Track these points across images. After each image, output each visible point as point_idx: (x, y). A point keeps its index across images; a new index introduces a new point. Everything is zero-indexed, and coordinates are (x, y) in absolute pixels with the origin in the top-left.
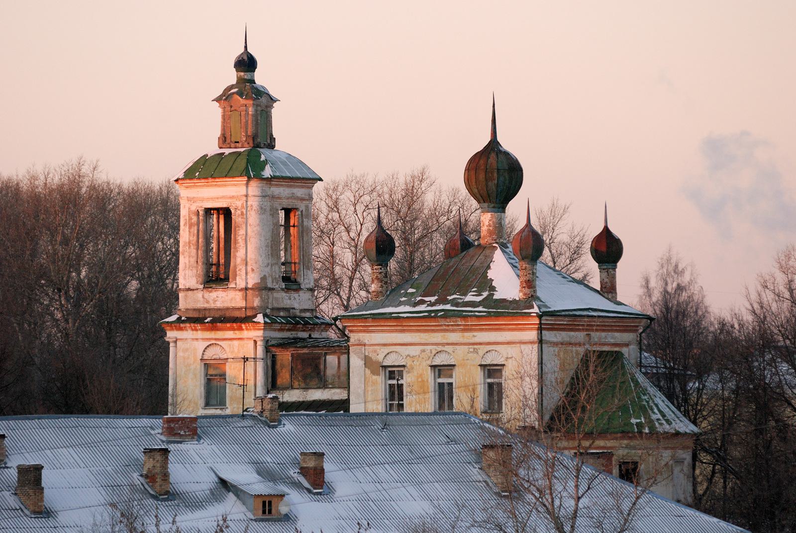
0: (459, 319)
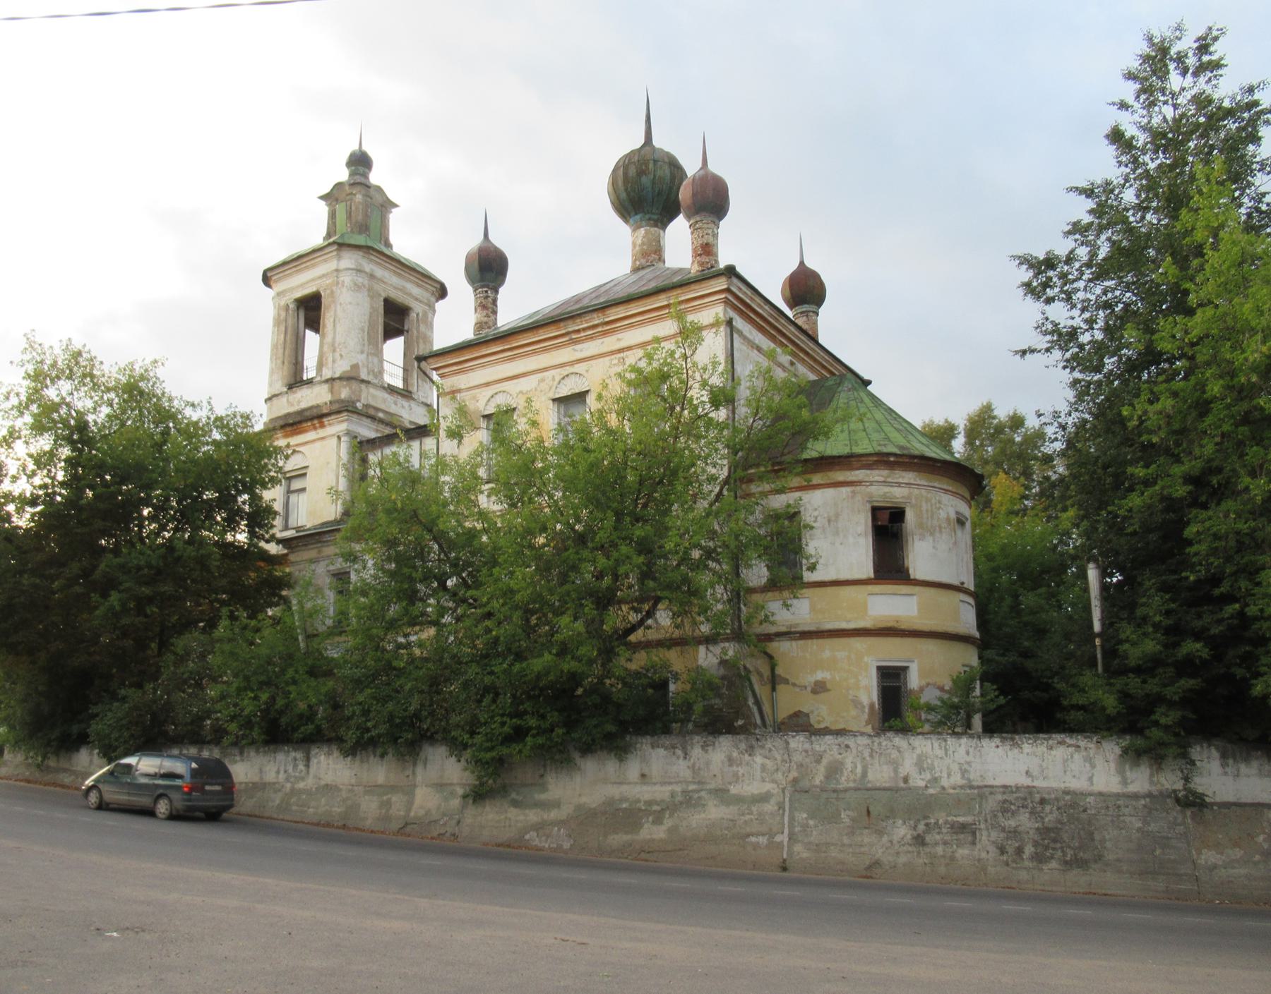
0: (595, 315)
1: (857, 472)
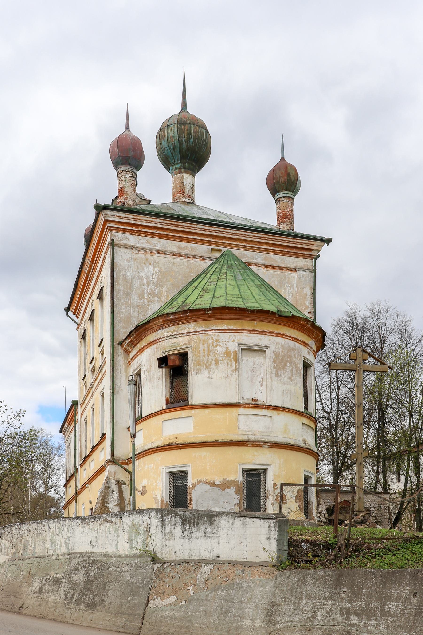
1: (158, 332)
